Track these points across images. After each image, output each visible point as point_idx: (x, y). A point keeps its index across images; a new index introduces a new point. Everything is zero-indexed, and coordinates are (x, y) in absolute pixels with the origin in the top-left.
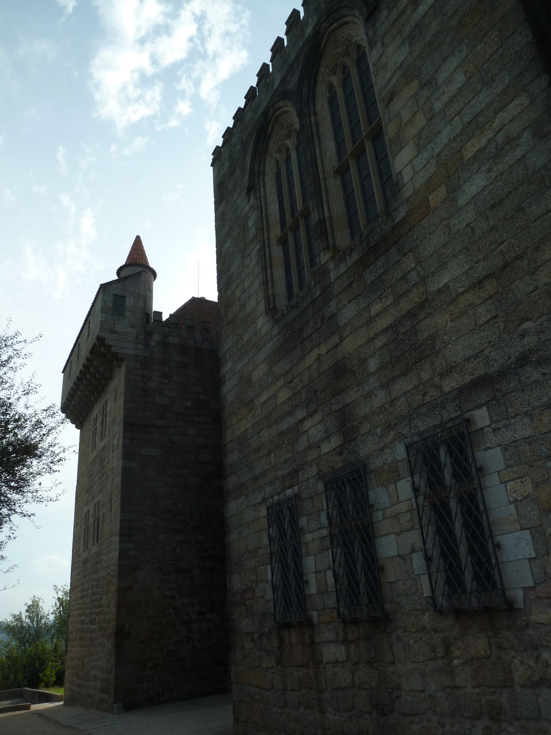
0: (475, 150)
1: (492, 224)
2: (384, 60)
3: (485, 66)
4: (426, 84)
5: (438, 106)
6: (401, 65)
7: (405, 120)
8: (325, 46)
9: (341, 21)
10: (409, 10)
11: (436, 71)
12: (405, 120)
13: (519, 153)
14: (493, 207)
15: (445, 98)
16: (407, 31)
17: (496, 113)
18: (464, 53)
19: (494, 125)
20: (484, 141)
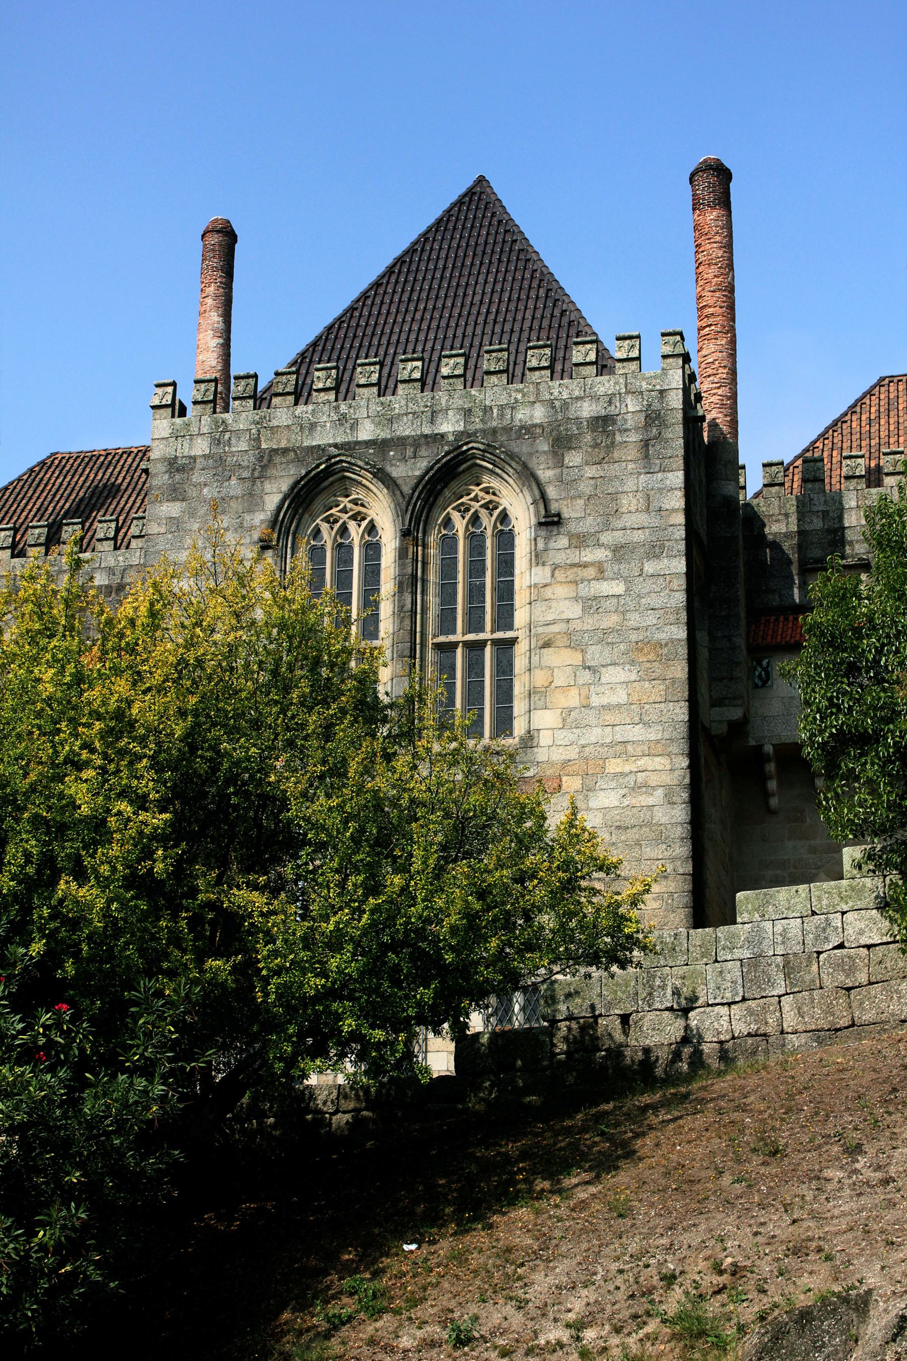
0: (619, 770)
1: (614, 840)
2: (548, 593)
3: (647, 707)
4: (589, 668)
5: (595, 701)
6: (568, 621)
7: (557, 683)
8: (463, 471)
9: (497, 470)
10: (591, 572)
11: (603, 666)
12: (557, 683)
13: (650, 801)
14: (618, 827)
15: (605, 701)
16: (584, 590)
17: (644, 755)
18: (633, 678)
19: (639, 763)
20: (627, 769)
